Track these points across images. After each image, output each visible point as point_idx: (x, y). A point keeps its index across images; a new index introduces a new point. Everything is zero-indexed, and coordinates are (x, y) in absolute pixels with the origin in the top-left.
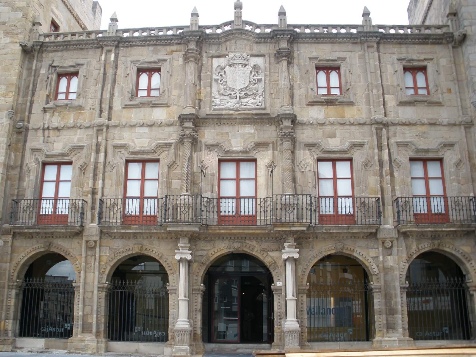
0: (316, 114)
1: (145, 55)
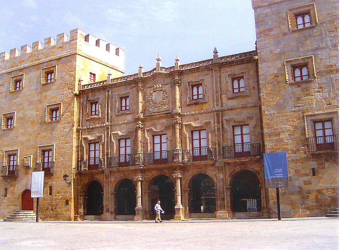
1: (123, 91)
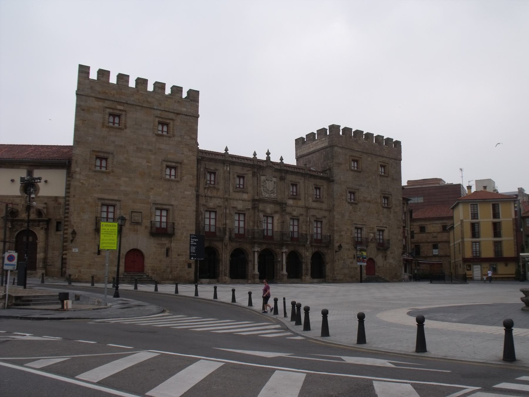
0: (290, 202)
